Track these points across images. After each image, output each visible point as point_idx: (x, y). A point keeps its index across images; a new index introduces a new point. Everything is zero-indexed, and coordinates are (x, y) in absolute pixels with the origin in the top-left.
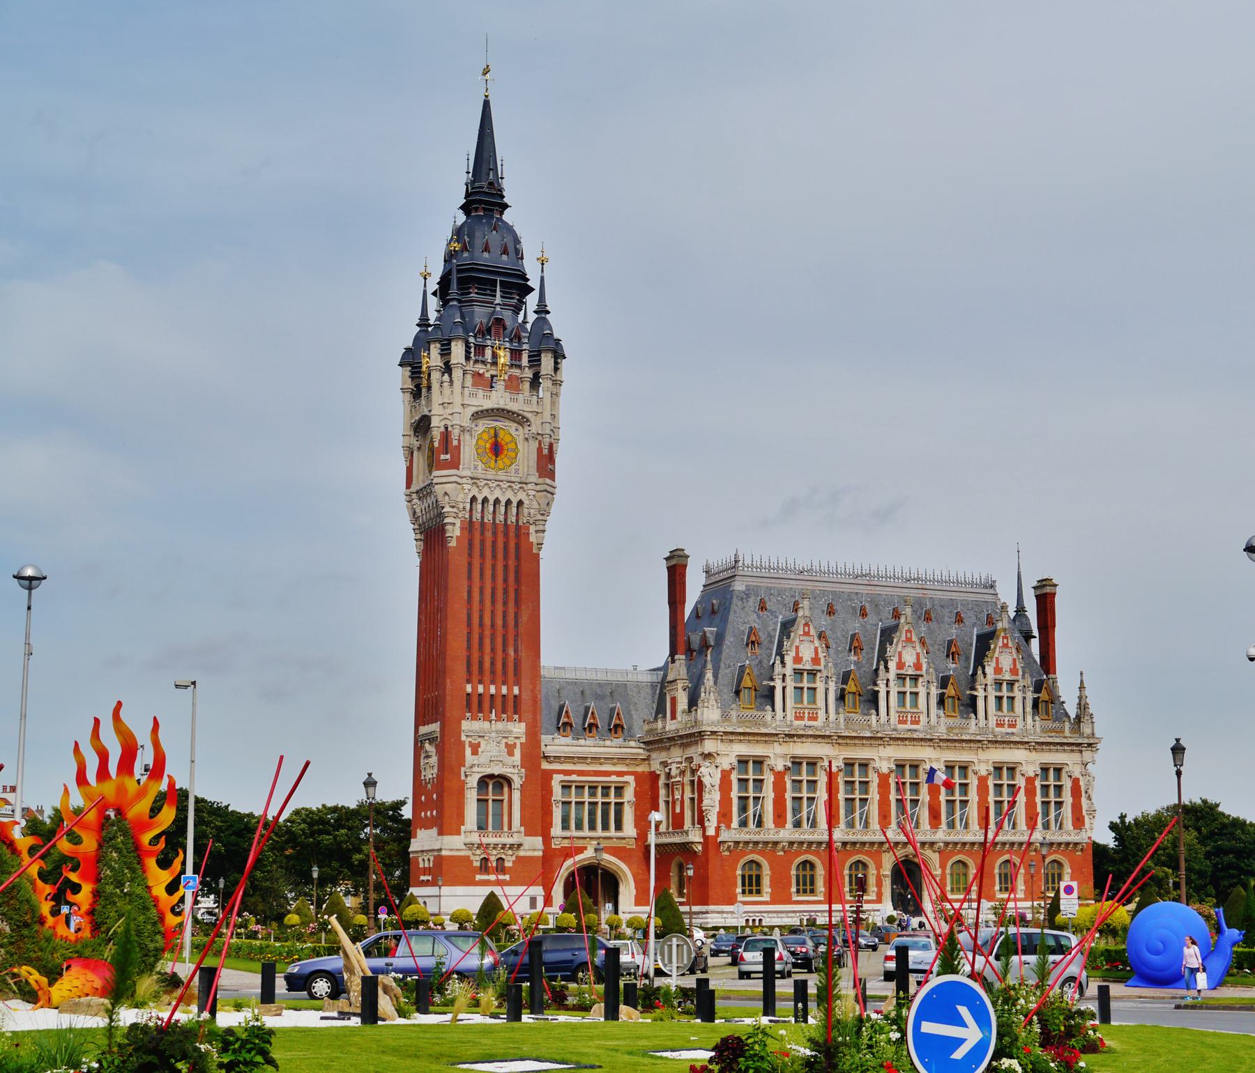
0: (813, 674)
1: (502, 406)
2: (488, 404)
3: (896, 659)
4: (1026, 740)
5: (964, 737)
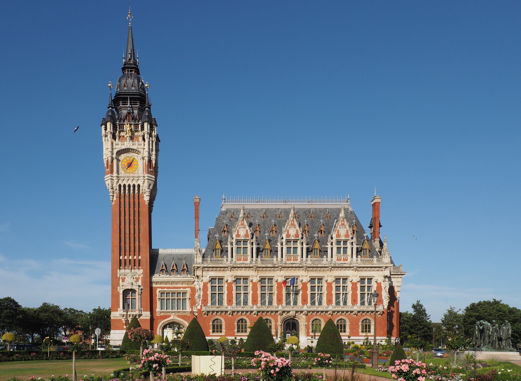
0: (245, 241)
1: (128, 147)
2: (123, 147)
3: (286, 233)
4: (351, 266)
5: (319, 266)
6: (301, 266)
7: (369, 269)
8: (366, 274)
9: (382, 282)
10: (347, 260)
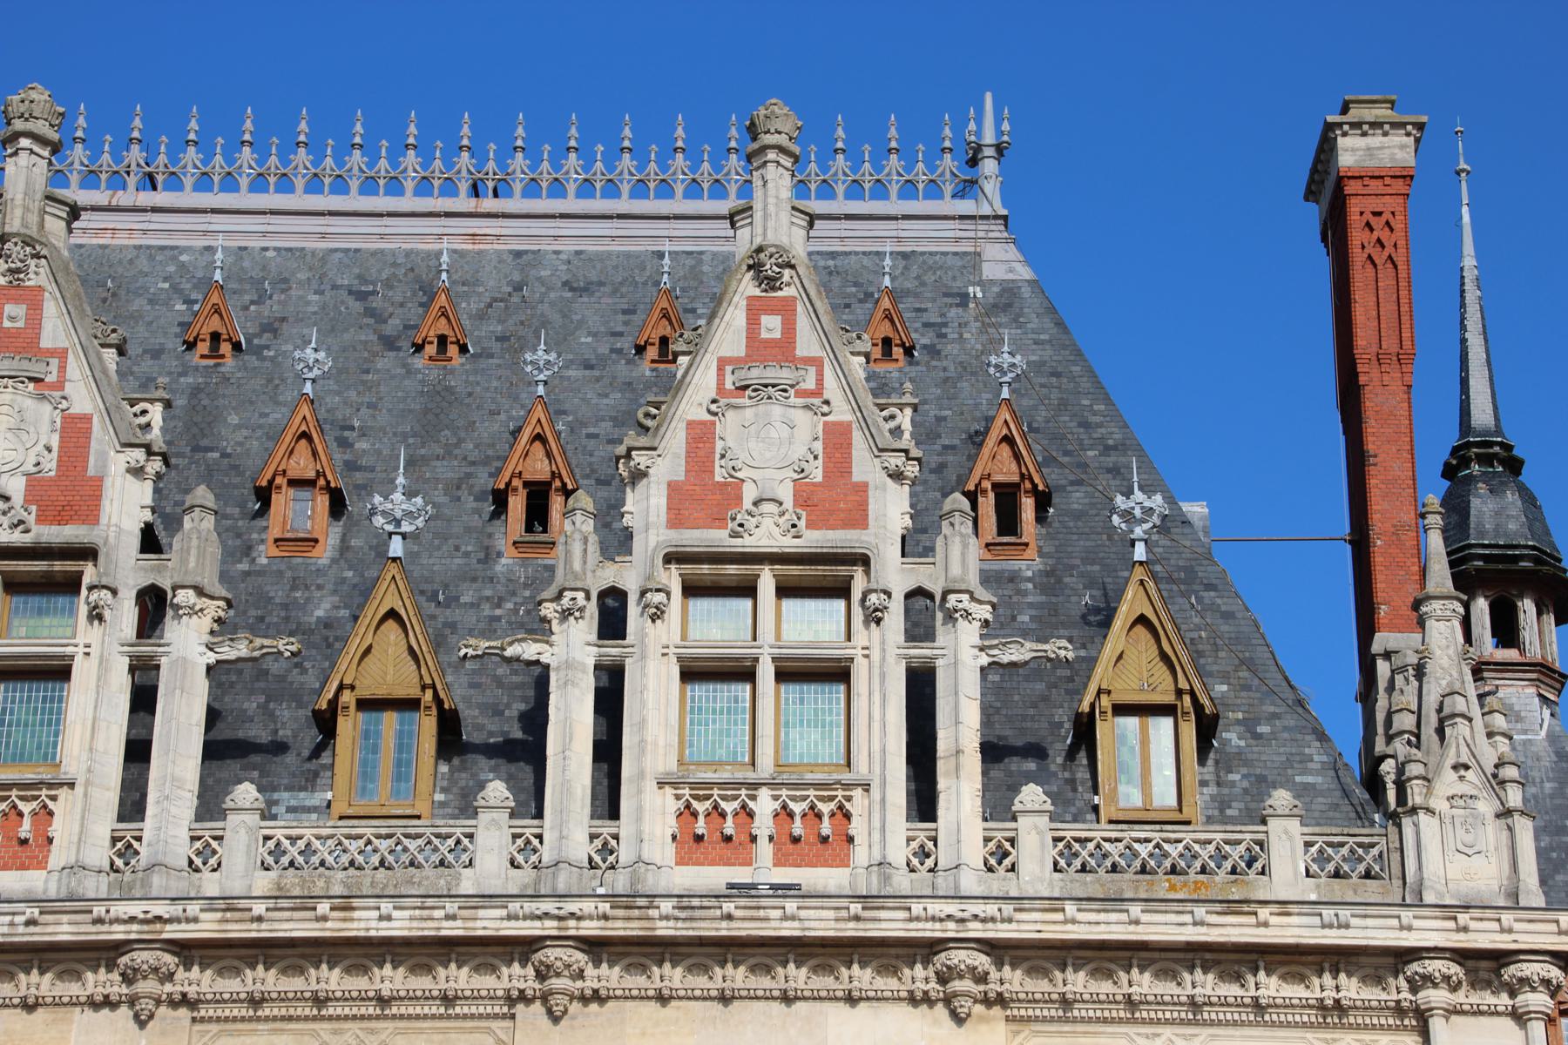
4: (890, 925)
5: (365, 923)
6: (64, 930)
10: (835, 844)
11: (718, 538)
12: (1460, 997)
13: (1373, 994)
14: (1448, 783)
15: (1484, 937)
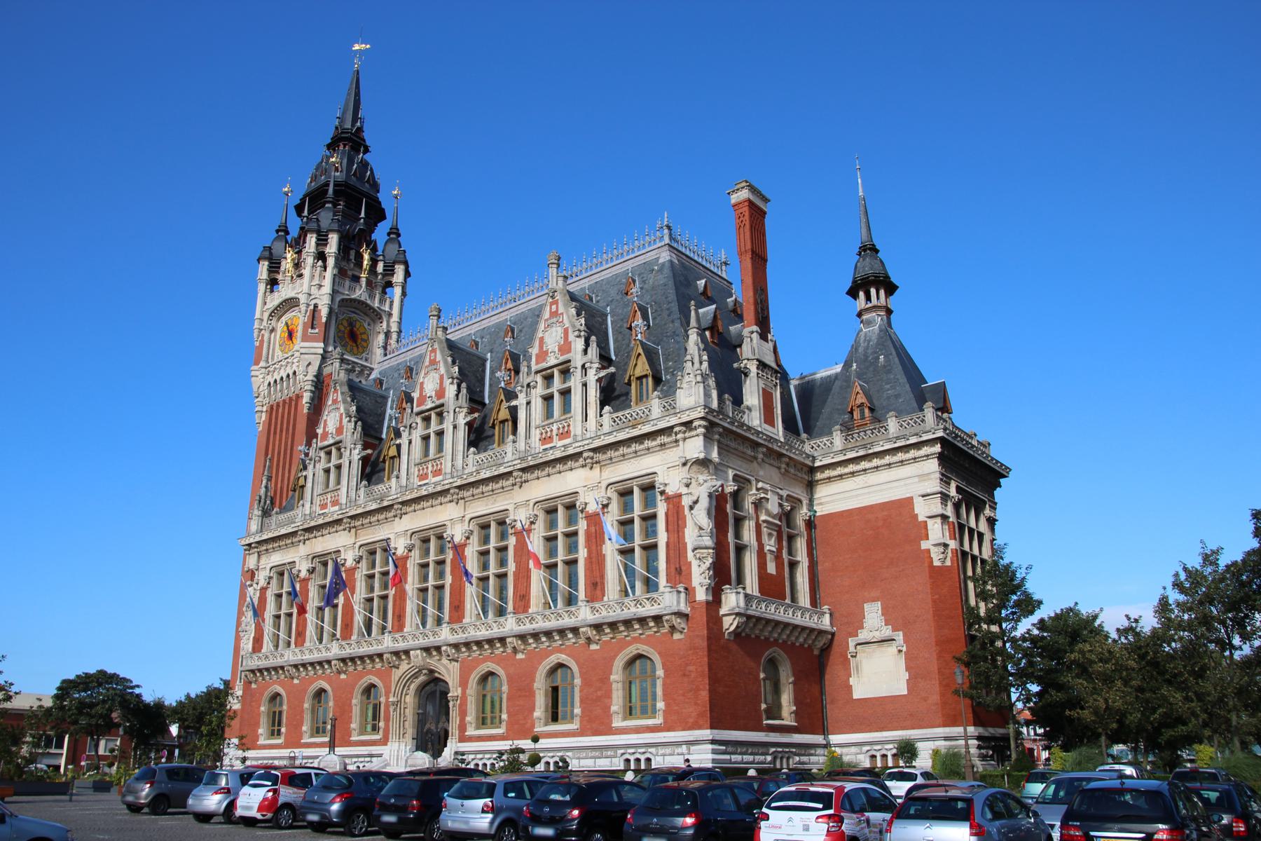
4: (571, 451)
7: (635, 447)
8: (630, 468)
9: (684, 490)
11: (544, 365)
12: (687, 435)
13: (670, 439)
14: (687, 378)
15: (685, 419)
